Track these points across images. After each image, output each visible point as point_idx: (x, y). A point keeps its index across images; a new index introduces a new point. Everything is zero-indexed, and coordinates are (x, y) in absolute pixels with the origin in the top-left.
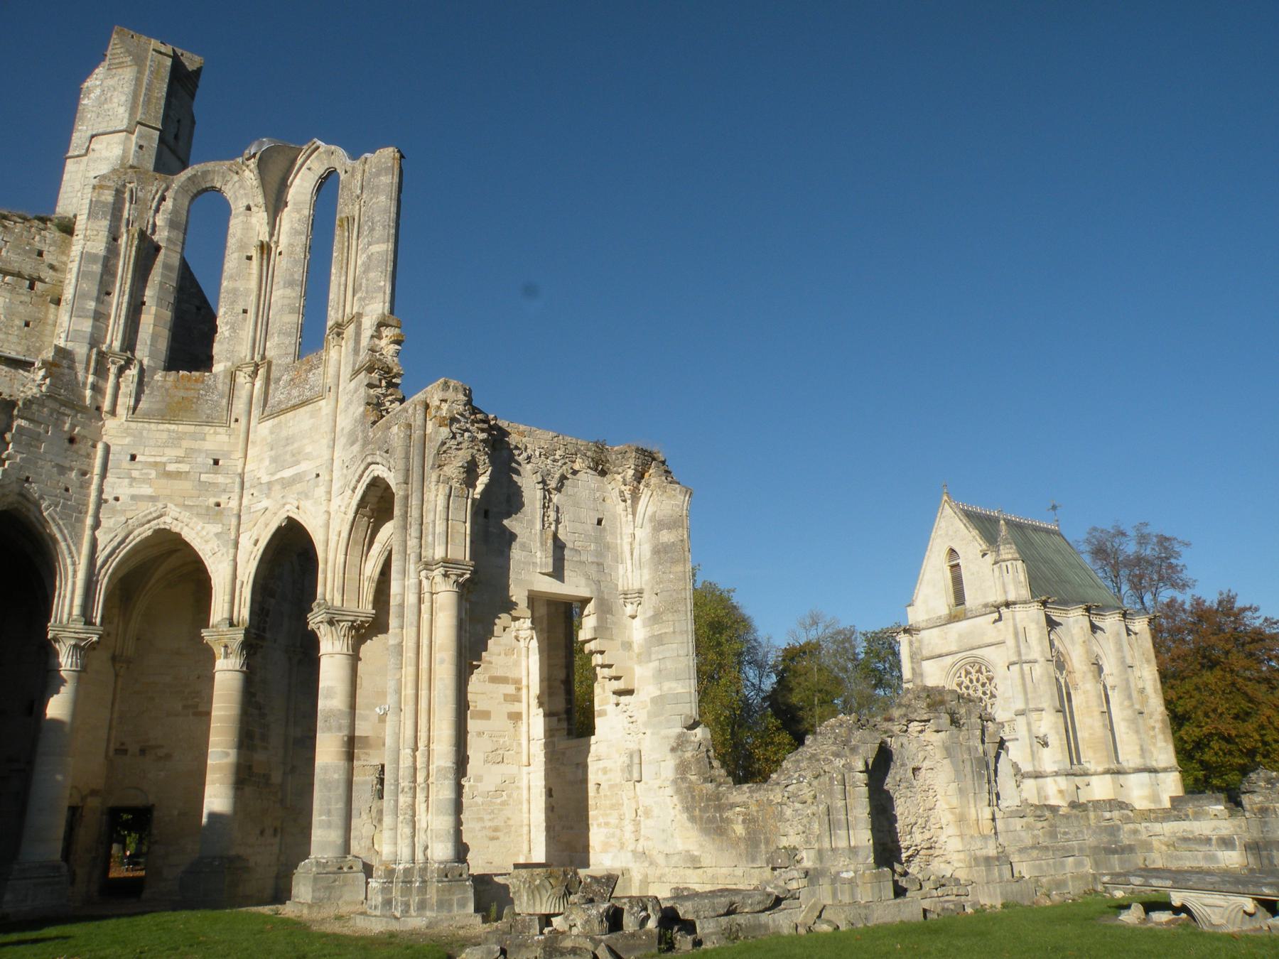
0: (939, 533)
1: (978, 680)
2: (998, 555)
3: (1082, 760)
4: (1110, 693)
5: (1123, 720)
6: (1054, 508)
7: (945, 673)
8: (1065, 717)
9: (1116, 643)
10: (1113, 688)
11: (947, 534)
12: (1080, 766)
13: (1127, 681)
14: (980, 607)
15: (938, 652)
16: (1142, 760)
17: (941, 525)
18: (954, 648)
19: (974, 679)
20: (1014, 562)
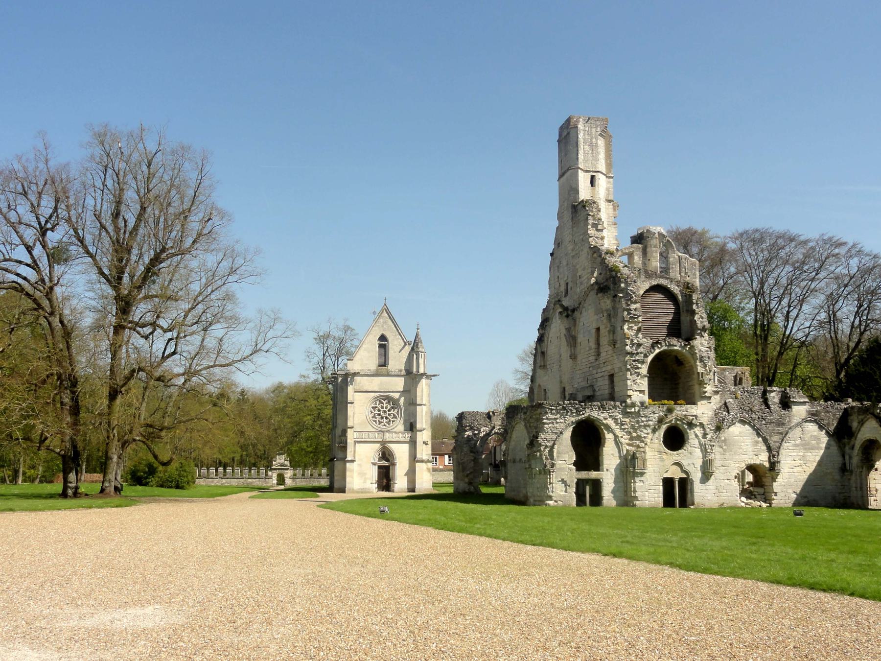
1: (386, 408)
11: (383, 326)
15: (365, 388)
18: (376, 389)
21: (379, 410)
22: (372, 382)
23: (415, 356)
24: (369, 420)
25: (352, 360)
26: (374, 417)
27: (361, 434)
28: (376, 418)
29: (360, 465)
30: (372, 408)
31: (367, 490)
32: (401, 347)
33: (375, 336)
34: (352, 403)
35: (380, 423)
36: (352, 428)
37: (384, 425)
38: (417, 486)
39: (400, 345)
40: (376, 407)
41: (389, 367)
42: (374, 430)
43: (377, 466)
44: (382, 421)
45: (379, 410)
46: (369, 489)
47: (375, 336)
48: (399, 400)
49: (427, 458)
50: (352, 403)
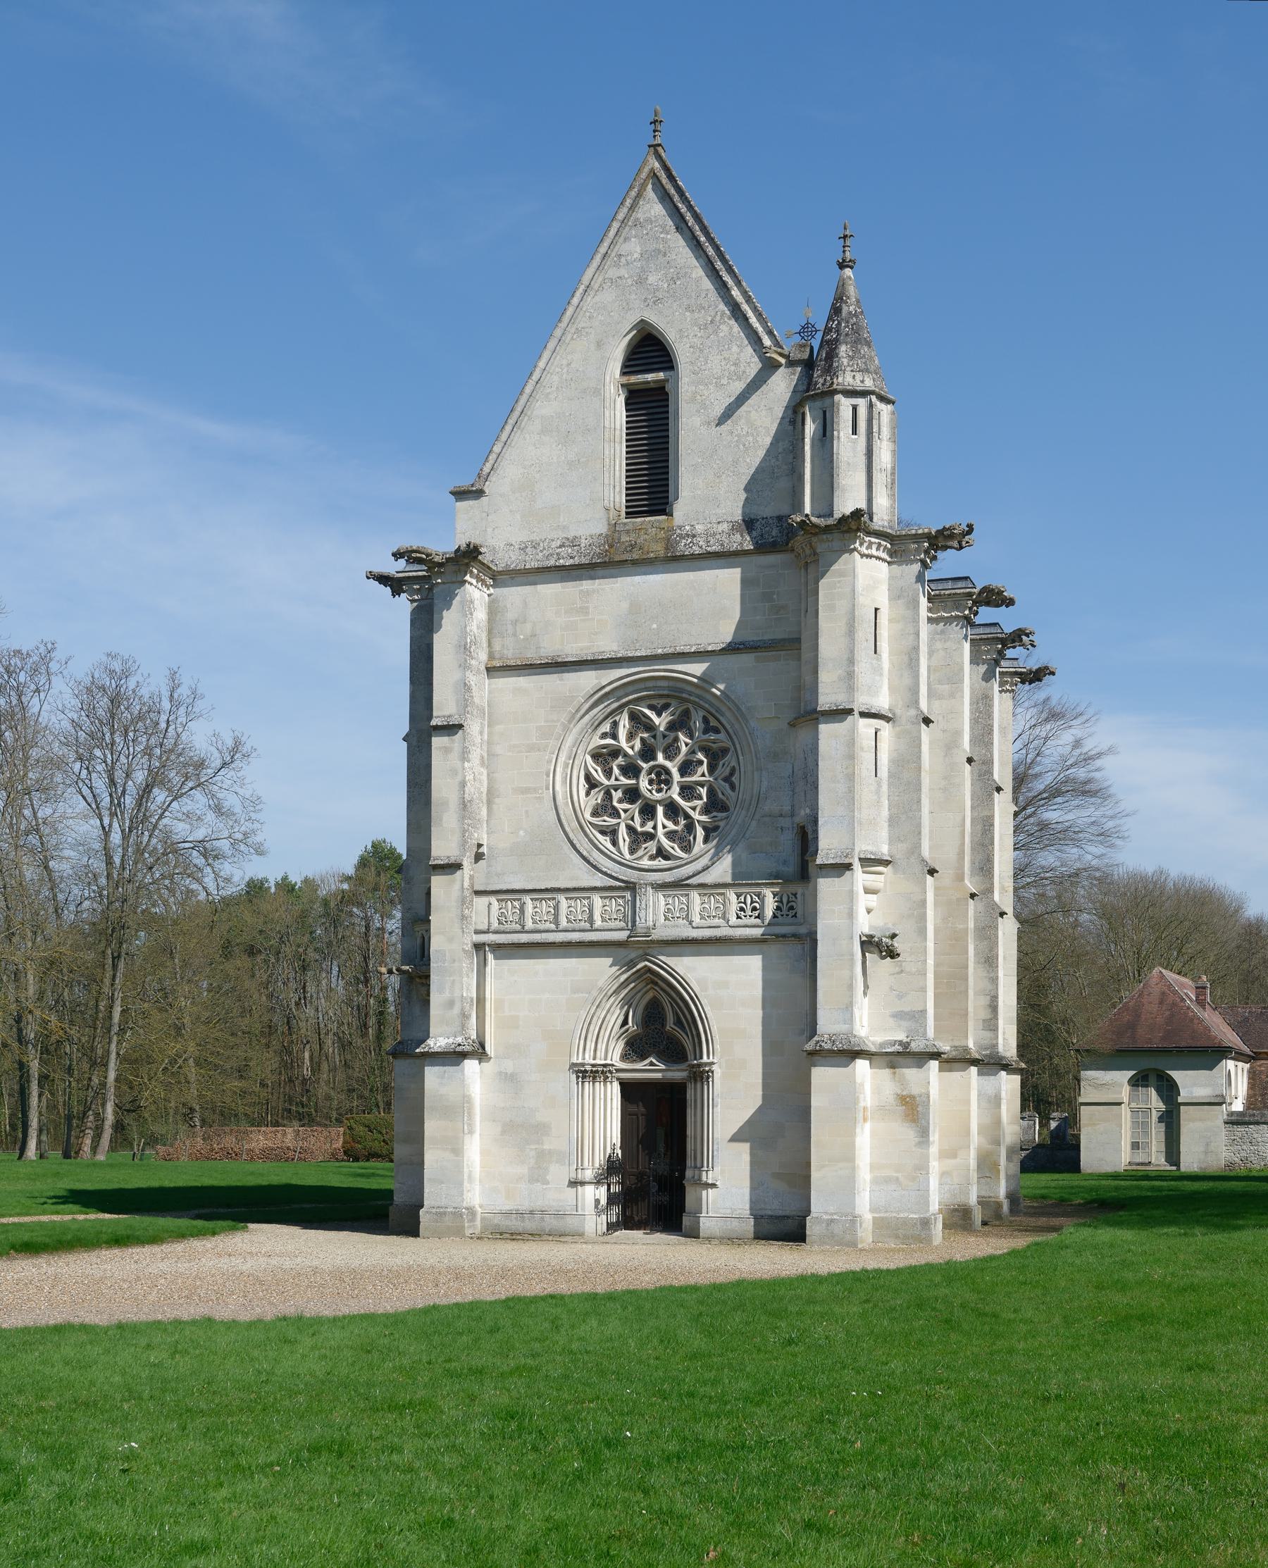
0: (612, 273)
7: (564, 718)
11: (641, 281)
15: (551, 647)
17: (623, 248)
18: (609, 646)
21: (631, 770)
22: (584, 610)
23: (810, 428)
24: (571, 825)
25: (479, 493)
26: (603, 809)
27: (511, 907)
28: (615, 813)
30: (596, 756)
33: (599, 345)
34: (452, 729)
35: (639, 839)
36: (452, 867)
37: (661, 853)
38: (818, 1205)
40: (616, 752)
41: (683, 511)
42: (599, 880)
43: (615, 1090)
44: (649, 827)
47: (599, 345)
49: (902, 1037)
50: (452, 729)
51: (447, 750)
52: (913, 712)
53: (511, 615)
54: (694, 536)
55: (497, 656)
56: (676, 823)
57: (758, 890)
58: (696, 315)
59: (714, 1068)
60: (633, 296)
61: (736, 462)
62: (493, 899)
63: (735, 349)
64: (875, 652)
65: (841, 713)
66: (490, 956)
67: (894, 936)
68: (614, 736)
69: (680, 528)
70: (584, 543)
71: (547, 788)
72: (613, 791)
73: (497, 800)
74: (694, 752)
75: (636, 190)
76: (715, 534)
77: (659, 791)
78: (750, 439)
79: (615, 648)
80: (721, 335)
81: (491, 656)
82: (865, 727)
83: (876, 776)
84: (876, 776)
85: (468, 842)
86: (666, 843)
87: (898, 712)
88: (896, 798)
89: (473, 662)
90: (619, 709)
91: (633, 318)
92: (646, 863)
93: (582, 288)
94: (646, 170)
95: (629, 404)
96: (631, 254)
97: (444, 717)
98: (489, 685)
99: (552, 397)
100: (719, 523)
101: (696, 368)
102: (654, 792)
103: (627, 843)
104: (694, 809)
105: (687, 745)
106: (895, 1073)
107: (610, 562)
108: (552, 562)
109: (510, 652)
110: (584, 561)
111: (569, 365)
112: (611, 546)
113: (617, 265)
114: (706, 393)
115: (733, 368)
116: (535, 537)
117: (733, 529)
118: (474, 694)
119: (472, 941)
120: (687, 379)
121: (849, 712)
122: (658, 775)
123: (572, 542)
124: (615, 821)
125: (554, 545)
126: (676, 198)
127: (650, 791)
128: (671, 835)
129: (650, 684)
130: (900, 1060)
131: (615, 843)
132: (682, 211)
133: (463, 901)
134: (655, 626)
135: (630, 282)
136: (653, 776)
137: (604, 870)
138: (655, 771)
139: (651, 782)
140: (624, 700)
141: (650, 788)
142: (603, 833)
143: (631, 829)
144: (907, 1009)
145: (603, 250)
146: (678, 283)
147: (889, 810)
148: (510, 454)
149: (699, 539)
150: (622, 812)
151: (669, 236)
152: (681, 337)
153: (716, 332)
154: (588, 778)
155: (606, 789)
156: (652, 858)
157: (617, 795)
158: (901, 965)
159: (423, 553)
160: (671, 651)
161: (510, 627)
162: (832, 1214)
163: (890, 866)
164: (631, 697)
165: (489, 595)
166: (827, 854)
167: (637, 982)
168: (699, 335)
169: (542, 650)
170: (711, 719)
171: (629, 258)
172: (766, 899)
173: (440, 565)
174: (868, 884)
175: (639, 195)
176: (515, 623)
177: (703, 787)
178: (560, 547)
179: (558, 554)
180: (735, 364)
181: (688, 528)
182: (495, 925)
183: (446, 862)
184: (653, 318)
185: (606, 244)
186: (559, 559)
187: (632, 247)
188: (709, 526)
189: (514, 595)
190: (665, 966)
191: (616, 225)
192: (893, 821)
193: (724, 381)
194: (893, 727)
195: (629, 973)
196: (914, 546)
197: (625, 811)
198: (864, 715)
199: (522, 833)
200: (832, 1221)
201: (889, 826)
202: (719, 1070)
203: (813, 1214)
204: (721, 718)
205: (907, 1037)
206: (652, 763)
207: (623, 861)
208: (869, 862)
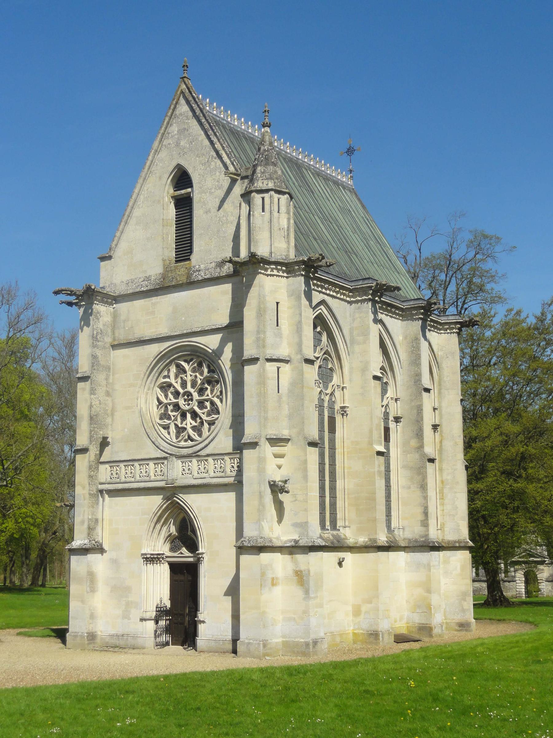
2: (252, 181)
3: (339, 523)
4: (392, 425)
5: (404, 467)
6: (350, 151)
8: (322, 455)
9: (412, 352)
10: (397, 420)
11: (178, 145)
12: (335, 532)
13: (420, 410)
14: (213, 265)
16: (423, 529)
17: (170, 129)
18: (164, 331)
19: (189, 379)
20: (276, 196)
21: (177, 394)
22: (153, 313)
25: (110, 258)
26: (165, 416)
28: (169, 418)
29: (115, 562)
31: (131, 641)
32: (221, 193)
33: (160, 178)
34: (85, 379)
35: (180, 430)
37: (190, 438)
39: (220, 188)
40: (170, 385)
41: (194, 257)
44: (184, 425)
45: (177, 394)
46: (135, 637)
47: (160, 178)
48: (218, 353)
49: (296, 537)
50: (85, 379)
51: (84, 389)
52: (299, 356)
53: (123, 318)
54: (200, 271)
55: (117, 339)
56: (196, 422)
57: (222, 457)
58: (201, 159)
59: (204, 556)
60: (175, 152)
61: (218, 231)
62: (107, 466)
63: (218, 174)
64: (277, 325)
65: (254, 360)
66: (106, 496)
67: (286, 482)
68: (169, 377)
69: (194, 267)
70: (153, 278)
71: (137, 406)
72: (168, 406)
73: (116, 413)
74: (204, 384)
75: (175, 100)
76: (209, 269)
77: (189, 405)
78: (224, 218)
79: (166, 331)
80: (212, 167)
81: (114, 340)
82: (271, 367)
83: (278, 392)
84: (278, 392)
85: (94, 437)
86: (191, 432)
87: (293, 357)
88: (292, 404)
89: (100, 343)
90: (171, 362)
91: (174, 164)
92: (183, 444)
93: (153, 151)
94: (180, 90)
95: (177, 206)
96: (173, 132)
97: (83, 372)
98: (113, 354)
99: (140, 206)
100: (211, 263)
101: (201, 185)
102: (186, 405)
103: (174, 434)
104: (203, 413)
105: (201, 380)
106: (292, 558)
107: (163, 287)
108: (138, 290)
109: (122, 336)
110: (152, 287)
111: (147, 190)
112: (164, 279)
113: (168, 138)
114: (205, 197)
115: (217, 183)
116: (133, 277)
117: (216, 266)
118: (100, 360)
119: (97, 489)
120: (197, 191)
121: (257, 359)
122: (188, 396)
123: (148, 278)
124: (169, 422)
125: (141, 280)
126: (192, 102)
127: (184, 405)
128: (194, 428)
129: (183, 349)
130: (295, 550)
131: (169, 433)
132: (194, 108)
133: (90, 467)
134: (183, 319)
135: (173, 145)
136: (186, 397)
137: (161, 448)
138: (187, 394)
139: (185, 400)
140: (172, 358)
141: (184, 403)
142: (164, 428)
143: (176, 425)
144: (299, 521)
145: (162, 131)
146: (193, 143)
147: (289, 410)
148: (124, 237)
149: (201, 272)
150: (172, 417)
151: (189, 121)
152: (195, 171)
153: (209, 166)
154: (158, 399)
155: (165, 405)
156: (186, 441)
157: (170, 408)
158: (296, 497)
159: (68, 291)
160: (189, 331)
161: (122, 324)
162: (250, 639)
163: (290, 443)
164: (174, 356)
165: (114, 308)
166: (248, 437)
167: (172, 509)
168: (202, 168)
169: (136, 335)
170: (211, 365)
171: (173, 134)
172: (226, 462)
173: (81, 295)
174: (275, 452)
175: (177, 103)
176: (124, 321)
177: (207, 401)
178: (143, 281)
179: (141, 285)
180: (218, 181)
181: (197, 267)
182: (109, 480)
183: (81, 447)
184: (183, 163)
185: (163, 128)
186: (142, 287)
187: (174, 129)
188: (207, 265)
189: (123, 307)
190: (182, 500)
191: (167, 119)
192: (290, 417)
193: (213, 191)
194: (290, 365)
195: (167, 504)
196: (296, 267)
197: (174, 416)
198: (269, 360)
199: (126, 430)
200: (249, 643)
201: (289, 419)
202: (207, 557)
203: (241, 640)
204: (214, 365)
205: (299, 537)
206: (186, 390)
207: (171, 443)
208: (274, 441)
